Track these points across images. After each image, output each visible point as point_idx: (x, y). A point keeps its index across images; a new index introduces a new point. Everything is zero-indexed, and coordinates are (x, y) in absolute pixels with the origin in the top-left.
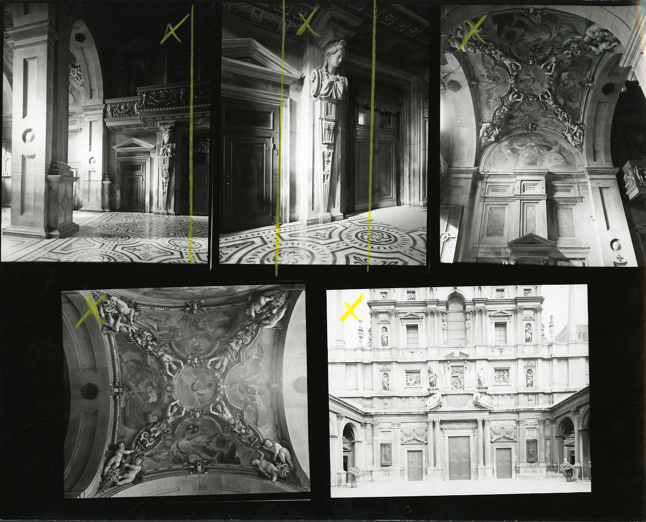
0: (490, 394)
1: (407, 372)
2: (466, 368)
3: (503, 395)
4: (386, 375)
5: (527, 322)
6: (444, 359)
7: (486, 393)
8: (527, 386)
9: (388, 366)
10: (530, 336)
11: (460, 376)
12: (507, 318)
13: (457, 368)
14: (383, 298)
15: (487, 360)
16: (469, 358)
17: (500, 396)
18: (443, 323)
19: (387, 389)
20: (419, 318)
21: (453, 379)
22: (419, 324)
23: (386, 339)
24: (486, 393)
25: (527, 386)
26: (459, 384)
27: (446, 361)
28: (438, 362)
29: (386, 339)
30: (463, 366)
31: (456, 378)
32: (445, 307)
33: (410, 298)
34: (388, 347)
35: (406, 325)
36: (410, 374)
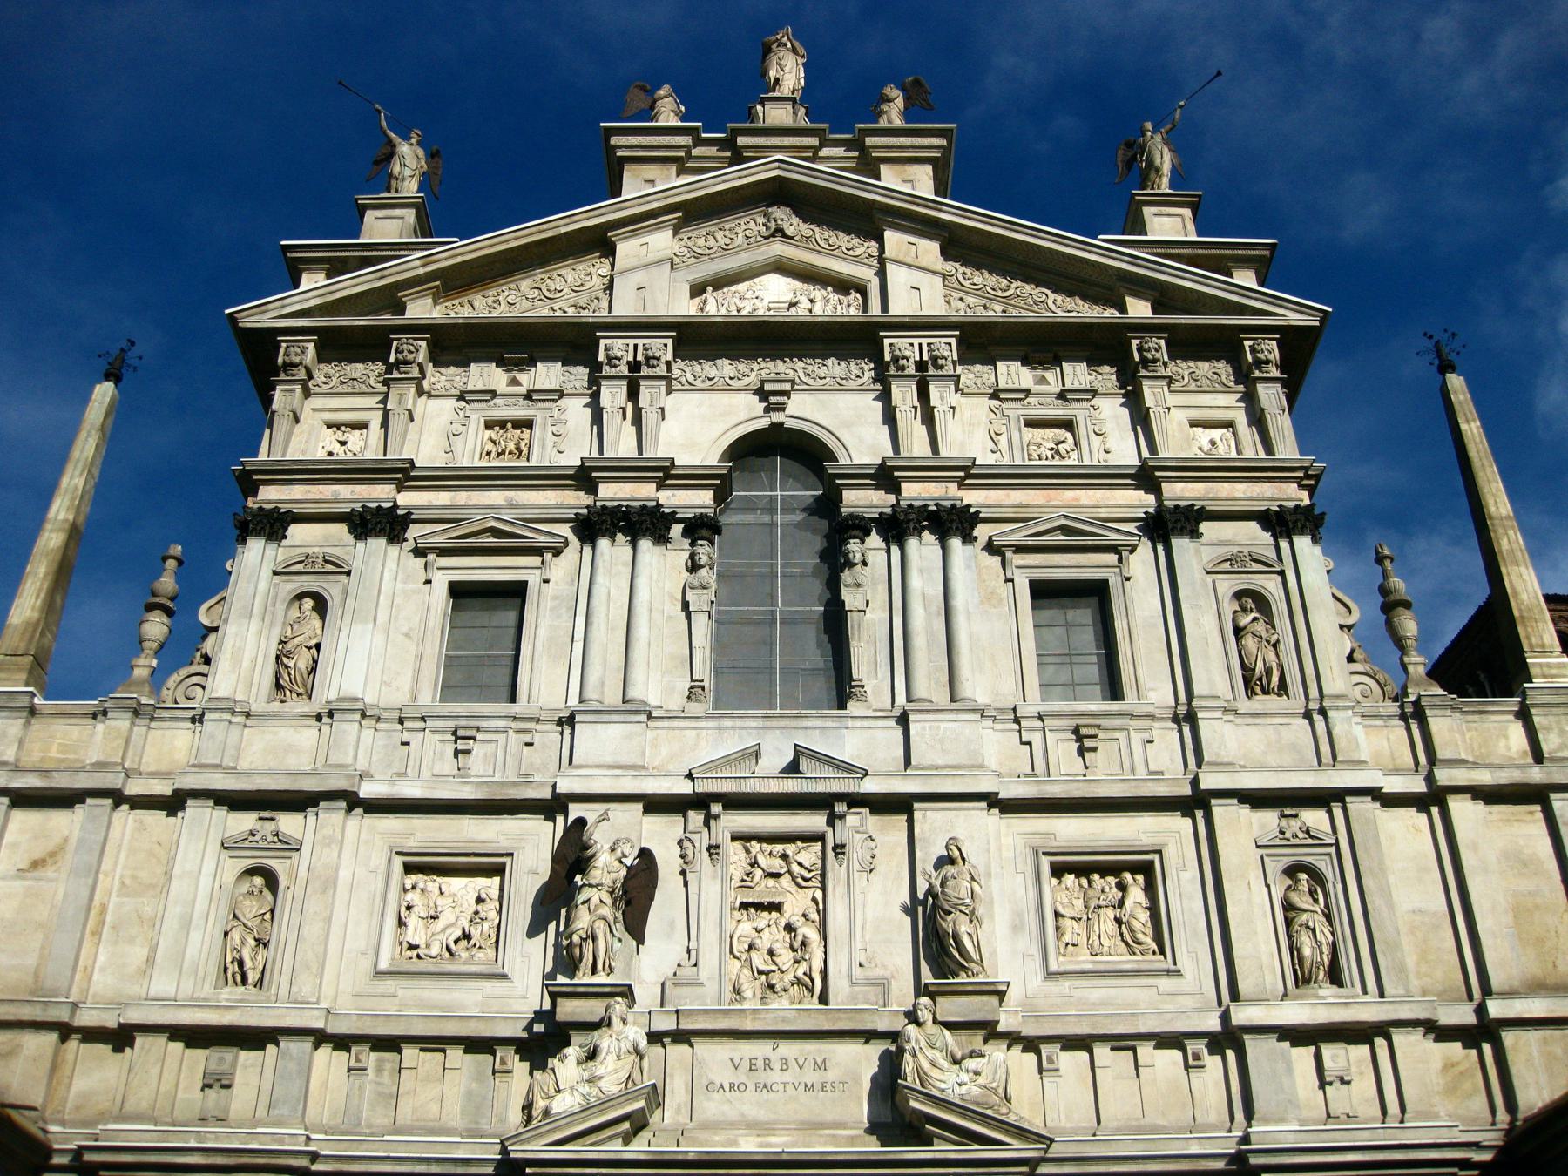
0: (1029, 1030)
1: (409, 869)
2: (839, 849)
3: (1123, 1042)
4: (258, 881)
5: (1243, 582)
6: (685, 788)
7: (990, 1030)
8: (1303, 978)
9: (289, 823)
10: (1271, 655)
11: (796, 903)
12: (1112, 558)
13: (778, 848)
14: (337, 448)
15: (992, 801)
16: (870, 786)
17: (1102, 1052)
18: (693, 579)
19: (252, 976)
20: (537, 551)
21: (746, 928)
22: (533, 579)
23: (302, 661)
24: (990, 1030)
25: (1303, 978)
26: (785, 958)
27: (700, 802)
28: (640, 806)
29: (302, 661)
30: (820, 838)
31: (764, 918)
32: (707, 497)
33: (494, 450)
34: (318, 704)
36: (432, 883)
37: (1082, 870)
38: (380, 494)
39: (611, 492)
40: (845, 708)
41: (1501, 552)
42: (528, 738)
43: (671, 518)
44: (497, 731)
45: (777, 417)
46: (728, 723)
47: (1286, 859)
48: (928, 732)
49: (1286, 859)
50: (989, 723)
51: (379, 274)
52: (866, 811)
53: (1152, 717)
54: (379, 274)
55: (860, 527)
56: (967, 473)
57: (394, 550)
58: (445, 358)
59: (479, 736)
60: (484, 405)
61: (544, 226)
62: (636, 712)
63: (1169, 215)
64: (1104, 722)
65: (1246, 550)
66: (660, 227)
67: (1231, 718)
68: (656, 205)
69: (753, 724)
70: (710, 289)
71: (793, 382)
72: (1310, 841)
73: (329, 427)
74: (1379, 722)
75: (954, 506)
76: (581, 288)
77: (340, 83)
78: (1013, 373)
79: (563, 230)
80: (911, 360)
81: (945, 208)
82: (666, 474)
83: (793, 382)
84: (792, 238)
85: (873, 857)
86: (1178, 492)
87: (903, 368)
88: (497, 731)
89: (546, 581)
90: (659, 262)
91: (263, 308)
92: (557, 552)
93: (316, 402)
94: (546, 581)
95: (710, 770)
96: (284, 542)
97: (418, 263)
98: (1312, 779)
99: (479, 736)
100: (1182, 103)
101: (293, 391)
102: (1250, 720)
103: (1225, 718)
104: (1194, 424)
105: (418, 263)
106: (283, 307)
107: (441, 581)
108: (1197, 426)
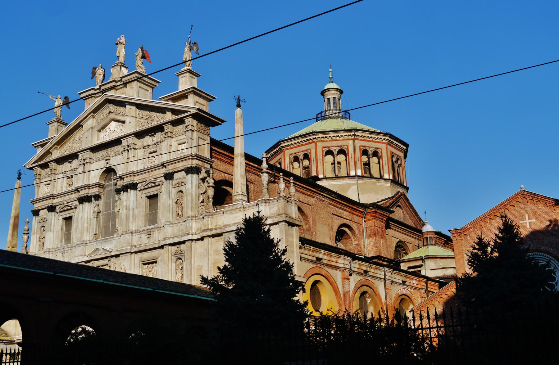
16: (113, 254)
35: (63, 218)
37: (149, 264)
38: (49, 203)
39: (83, 193)
40: (113, 235)
41: (235, 165)
42: (72, 251)
43: (91, 197)
44: (67, 250)
45: (108, 166)
46: (98, 242)
47: (177, 257)
48: (123, 239)
49: (177, 257)
50: (135, 234)
51: (44, 149)
52: (114, 258)
53: (160, 227)
54: (44, 149)
55: (118, 191)
56: (134, 174)
57: (53, 213)
58: (60, 164)
59: (65, 252)
60: (66, 174)
61: (76, 121)
62: (83, 243)
63: (184, 77)
64: (151, 230)
65: (180, 180)
66: (89, 118)
67: (171, 225)
68: (86, 115)
69: (101, 241)
70: (102, 130)
71: (109, 156)
72: (182, 252)
73: (46, 185)
74: (199, 220)
75: (133, 183)
76: (80, 138)
77: (38, 92)
78: (148, 140)
79: (72, 127)
80: (126, 146)
81: (132, 99)
82: (88, 187)
83: (109, 156)
84: (113, 112)
85: (116, 267)
86: (170, 168)
87: (124, 148)
88: (67, 250)
89: (75, 215)
90: (89, 129)
91: (28, 163)
92: (76, 208)
93: (42, 181)
94: (75, 215)
95: (90, 255)
96: (40, 215)
97: (50, 144)
98: (178, 239)
99: (65, 252)
100: (189, 36)
101: (37, 181)
102: (175, 225)
103: (170, 226)
104: (179, 145)
105: (50, 144)
106: (32, 162)
107: (61, 218)
108: (180, 144)
